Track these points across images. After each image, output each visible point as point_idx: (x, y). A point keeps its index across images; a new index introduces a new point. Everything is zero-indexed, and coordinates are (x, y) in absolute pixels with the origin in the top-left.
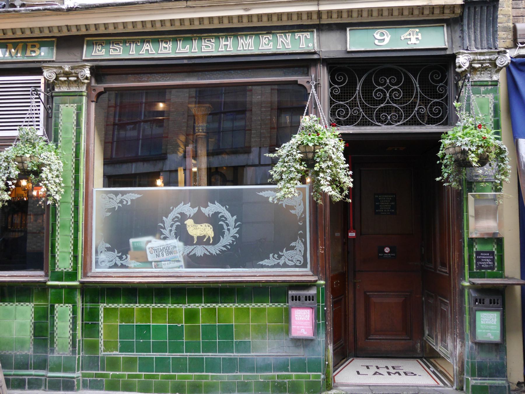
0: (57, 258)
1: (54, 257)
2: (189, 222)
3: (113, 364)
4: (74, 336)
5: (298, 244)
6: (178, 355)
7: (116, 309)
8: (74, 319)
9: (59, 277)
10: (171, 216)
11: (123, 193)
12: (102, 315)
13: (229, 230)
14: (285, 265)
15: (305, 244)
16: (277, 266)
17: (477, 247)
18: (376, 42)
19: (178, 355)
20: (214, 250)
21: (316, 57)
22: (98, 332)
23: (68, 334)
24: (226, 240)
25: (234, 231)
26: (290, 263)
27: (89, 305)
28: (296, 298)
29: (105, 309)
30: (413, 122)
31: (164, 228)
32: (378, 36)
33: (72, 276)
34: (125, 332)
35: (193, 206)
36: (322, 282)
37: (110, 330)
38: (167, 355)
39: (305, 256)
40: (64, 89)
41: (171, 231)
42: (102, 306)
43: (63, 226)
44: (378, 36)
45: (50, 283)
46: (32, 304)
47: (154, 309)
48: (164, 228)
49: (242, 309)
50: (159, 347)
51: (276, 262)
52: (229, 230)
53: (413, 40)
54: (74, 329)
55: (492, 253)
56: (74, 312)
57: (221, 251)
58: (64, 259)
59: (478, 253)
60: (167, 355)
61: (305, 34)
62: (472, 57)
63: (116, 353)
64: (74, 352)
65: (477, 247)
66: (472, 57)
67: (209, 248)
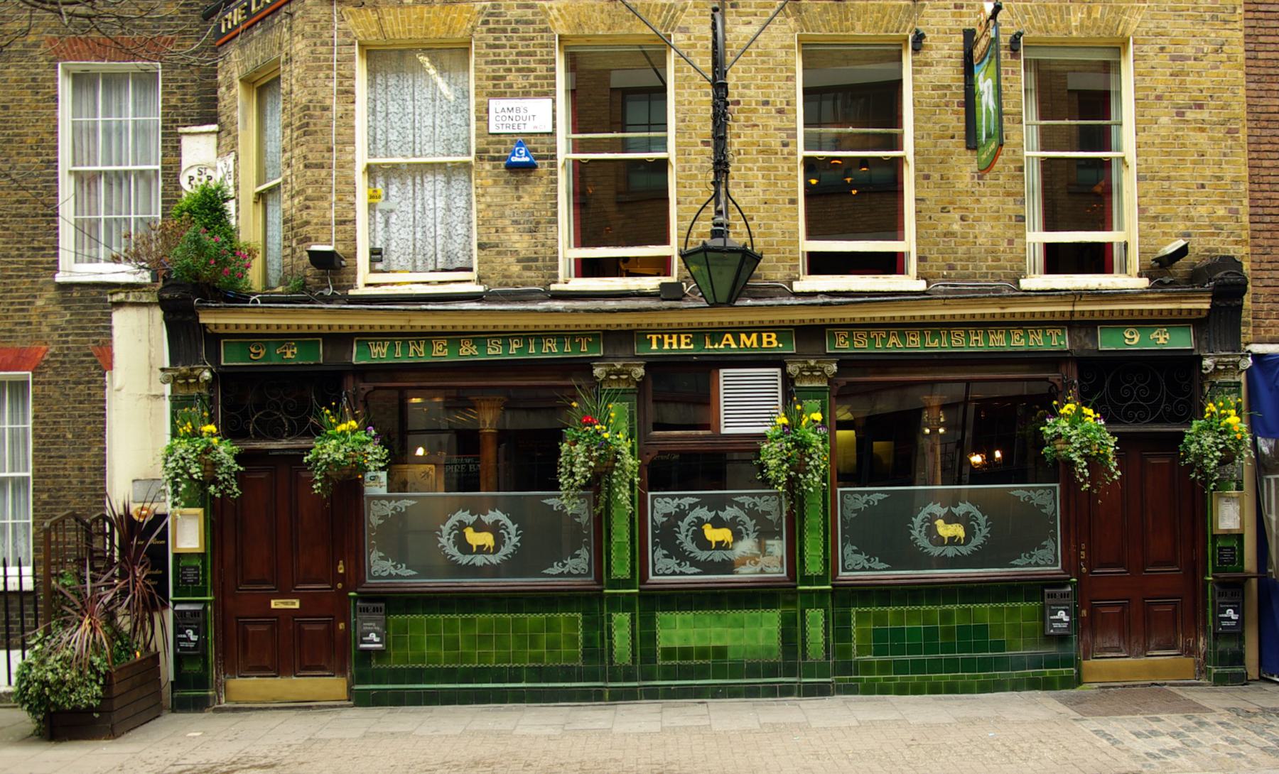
0: (807, 561)
1: (802, 561)
2: (940, 523)
3: (867, 667)
4: (827, 641)
5: (1049, 543)
6: (933, 656)
7: (869, 612)
8: (826, 623)
9: (807, 580)
10: (920, 516)
11: (870, 493)
12: (854, 619)
13: (980, 530)
14: (1037, 565)
15: (1056, 543)
16: (1029, 565)
17: (1220, 544)
18: (1126, 341)
19: (933, 656)
20: (965, 550)
21: (1069, 355)
22: (851, 636)
23: (821, 639)
24: (978, 540)
25: (985, 531)
26: (1042, 562)
27: (840, 610)
28: (1052, 596)
29: (857, 612)
30: (1159, 421)
31: (913, 529)
32: (1128, 336)
33: (820, 580)
34: (879, 635)
35: (942, 506)
36: (1074, 580)
37: (862, 633)
38: (922, 657)
39: (1056, 555)
40: (806, 384)
41: (920, 531)
42: (853, 610)
43: (812, 530)
44: (1128, 336)
45: (800, 588)
46: (779, 611)
47: (908, 611)
48: (913, 529)
49: (997, 608)
50: (914, 649)
51: (1028, 561)
52: (980, 530)
53: (1162, 341)
54: (826, 634)
55: (1233, 549)
56: (826, 617)
57: (973, 551)
58: (814, 563)
59: (1221, 549)
60: (922, 657)
61: (1056, 331)
62: (1216, 359)
63: (869, 657)
64: (827, 657)
65: (1220, 544)
66: (1216, 359)
67: (960, 548)
